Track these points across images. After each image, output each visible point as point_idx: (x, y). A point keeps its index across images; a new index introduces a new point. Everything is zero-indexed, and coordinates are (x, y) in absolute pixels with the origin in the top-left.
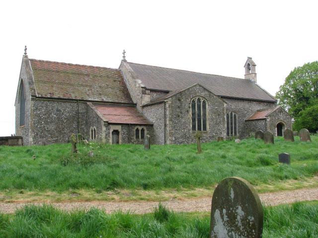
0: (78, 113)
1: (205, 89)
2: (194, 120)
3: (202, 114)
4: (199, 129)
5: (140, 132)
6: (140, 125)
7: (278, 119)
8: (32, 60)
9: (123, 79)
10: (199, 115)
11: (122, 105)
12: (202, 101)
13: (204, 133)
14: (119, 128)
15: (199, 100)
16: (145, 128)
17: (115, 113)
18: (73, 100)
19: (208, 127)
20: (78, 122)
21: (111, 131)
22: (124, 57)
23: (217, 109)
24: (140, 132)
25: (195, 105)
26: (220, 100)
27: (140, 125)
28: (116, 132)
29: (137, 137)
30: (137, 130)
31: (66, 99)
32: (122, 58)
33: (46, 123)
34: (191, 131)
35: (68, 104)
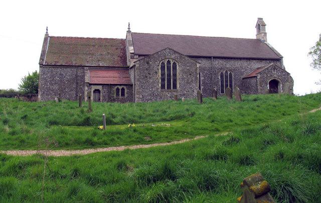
0: (77, 76)
1: (175, 52)
2: (163, 80)
3: (172, 74)
4: (169, 87)
5: (120, 92)
6: (120, 85)
7: (272, 76)
8: (51, 37)
9: (125, 47)
10: (169, 75)
11: (117, 68)
12: (172, 63)
13: (174, 91)
14: (100, 88)
15: (169, 62)
16: (125, 87)
17: (112, 75)
18: (73, 66)
19: (178, 86)
20: (77, 83)
21: (92, 91)
22: (129, 28)
23: (188, 69)
24: (120, 90)
25: (164, 67)
26: (192, 61)
27: (120, 85)
28: (97, 91)
29: (118, 94)
30: (118, 89)
31: (67, 66)
32: (127, 30)
33: (52, 84)
34: (159, 90)
35: (69, 70)
